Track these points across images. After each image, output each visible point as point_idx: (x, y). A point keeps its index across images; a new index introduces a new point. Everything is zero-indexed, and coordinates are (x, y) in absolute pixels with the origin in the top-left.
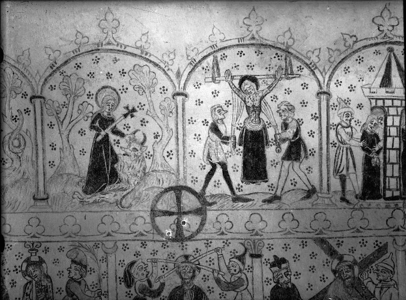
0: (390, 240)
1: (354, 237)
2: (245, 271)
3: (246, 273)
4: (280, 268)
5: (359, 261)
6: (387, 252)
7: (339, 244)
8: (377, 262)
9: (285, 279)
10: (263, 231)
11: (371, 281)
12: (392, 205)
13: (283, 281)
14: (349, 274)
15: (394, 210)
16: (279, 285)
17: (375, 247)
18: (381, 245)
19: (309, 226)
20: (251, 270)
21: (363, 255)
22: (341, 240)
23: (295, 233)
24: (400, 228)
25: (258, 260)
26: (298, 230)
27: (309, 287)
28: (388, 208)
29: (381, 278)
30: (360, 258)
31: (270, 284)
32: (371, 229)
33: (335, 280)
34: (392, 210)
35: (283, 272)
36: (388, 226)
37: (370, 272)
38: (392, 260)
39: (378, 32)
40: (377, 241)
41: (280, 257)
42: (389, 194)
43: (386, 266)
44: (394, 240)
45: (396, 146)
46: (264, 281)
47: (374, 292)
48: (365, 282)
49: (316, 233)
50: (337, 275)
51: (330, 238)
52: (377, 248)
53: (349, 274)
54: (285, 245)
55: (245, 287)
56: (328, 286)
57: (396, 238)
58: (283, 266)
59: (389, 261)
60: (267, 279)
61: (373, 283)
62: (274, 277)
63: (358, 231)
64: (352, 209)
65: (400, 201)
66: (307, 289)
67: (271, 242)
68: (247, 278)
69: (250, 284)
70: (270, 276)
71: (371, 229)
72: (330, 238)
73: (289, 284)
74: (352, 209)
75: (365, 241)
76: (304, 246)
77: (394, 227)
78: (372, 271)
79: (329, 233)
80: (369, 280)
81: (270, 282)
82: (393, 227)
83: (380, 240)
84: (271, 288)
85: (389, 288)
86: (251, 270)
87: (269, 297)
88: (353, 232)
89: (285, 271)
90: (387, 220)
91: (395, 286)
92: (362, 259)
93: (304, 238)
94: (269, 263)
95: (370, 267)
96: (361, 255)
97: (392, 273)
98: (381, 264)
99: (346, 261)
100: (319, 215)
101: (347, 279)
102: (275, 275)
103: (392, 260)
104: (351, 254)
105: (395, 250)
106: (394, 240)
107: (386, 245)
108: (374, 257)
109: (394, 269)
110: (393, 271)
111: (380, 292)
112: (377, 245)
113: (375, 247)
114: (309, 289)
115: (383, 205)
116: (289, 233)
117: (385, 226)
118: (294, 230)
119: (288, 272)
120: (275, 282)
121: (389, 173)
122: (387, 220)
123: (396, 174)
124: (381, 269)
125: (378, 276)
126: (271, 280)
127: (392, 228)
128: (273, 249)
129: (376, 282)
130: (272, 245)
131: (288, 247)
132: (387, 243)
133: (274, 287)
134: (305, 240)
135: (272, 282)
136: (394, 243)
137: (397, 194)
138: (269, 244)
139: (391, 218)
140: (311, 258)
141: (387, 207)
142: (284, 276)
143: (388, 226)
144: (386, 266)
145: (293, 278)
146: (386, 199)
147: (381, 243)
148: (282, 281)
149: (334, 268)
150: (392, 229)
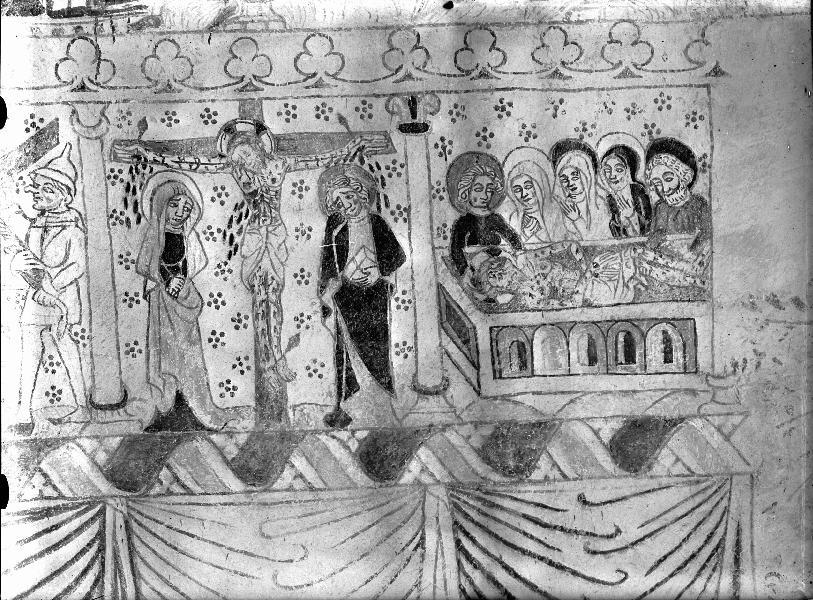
0: (62, 114)
6: (58, 143)
12: (69, 30)
15: (73, 42)
18: (42, 126)
24: (88, 84)
28: (58, 36)
29: (43, 204)
34: (68, 41)
38: (70, 162)
43: (56, 176)
44: (74, 112)
52: (33, 132)
59: (62, 164)
65: (86, 18)
83: (39, 112)
85: (64, 228)
90: (57, 65)
91: (80, 225)
97: (69, 193)
98: (42, 172)
103: (70, 162)
105: (76, 136)
107: (55, 124)
108: (27, 155)
109: (74, 183)
110: (73, 188)
111: (43, 239)
115: (47, 30)
122: (57, 65)
124: (41, 181)
125: (37, 199)
129: (33, 214)
132: (57, 119)
136: (75, 120)
139: (65, 59)
141: (57, 34)
144: (56, 176)
147: (42, 120)
150: (68, 88)
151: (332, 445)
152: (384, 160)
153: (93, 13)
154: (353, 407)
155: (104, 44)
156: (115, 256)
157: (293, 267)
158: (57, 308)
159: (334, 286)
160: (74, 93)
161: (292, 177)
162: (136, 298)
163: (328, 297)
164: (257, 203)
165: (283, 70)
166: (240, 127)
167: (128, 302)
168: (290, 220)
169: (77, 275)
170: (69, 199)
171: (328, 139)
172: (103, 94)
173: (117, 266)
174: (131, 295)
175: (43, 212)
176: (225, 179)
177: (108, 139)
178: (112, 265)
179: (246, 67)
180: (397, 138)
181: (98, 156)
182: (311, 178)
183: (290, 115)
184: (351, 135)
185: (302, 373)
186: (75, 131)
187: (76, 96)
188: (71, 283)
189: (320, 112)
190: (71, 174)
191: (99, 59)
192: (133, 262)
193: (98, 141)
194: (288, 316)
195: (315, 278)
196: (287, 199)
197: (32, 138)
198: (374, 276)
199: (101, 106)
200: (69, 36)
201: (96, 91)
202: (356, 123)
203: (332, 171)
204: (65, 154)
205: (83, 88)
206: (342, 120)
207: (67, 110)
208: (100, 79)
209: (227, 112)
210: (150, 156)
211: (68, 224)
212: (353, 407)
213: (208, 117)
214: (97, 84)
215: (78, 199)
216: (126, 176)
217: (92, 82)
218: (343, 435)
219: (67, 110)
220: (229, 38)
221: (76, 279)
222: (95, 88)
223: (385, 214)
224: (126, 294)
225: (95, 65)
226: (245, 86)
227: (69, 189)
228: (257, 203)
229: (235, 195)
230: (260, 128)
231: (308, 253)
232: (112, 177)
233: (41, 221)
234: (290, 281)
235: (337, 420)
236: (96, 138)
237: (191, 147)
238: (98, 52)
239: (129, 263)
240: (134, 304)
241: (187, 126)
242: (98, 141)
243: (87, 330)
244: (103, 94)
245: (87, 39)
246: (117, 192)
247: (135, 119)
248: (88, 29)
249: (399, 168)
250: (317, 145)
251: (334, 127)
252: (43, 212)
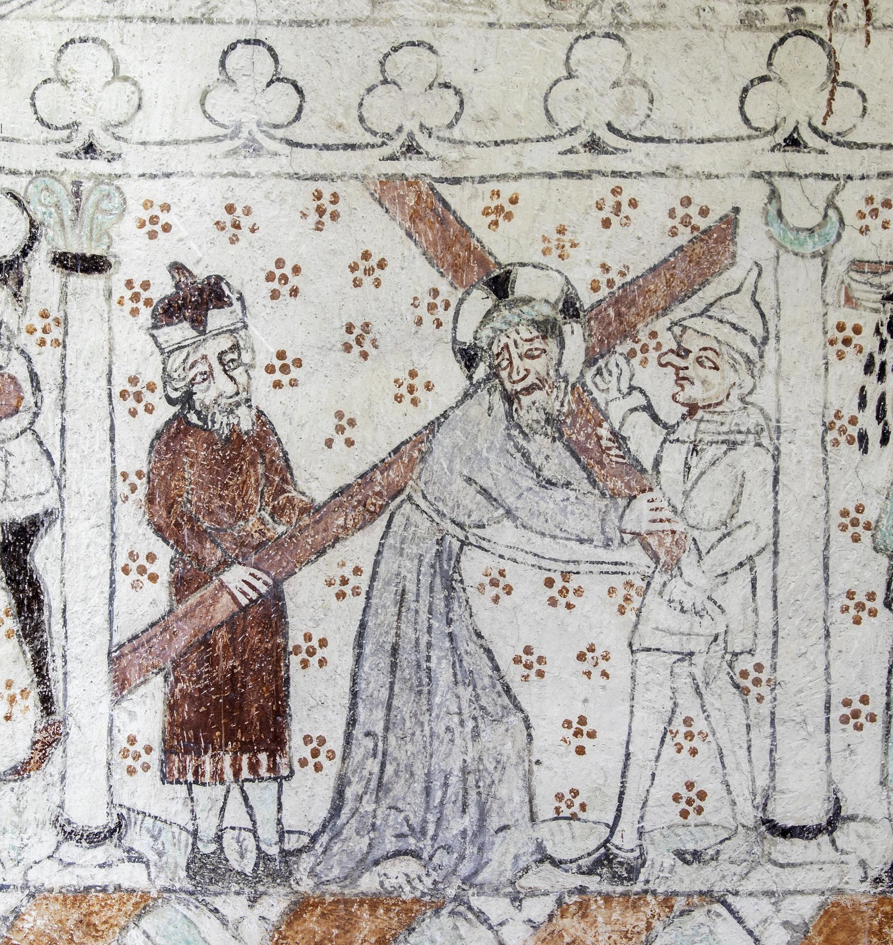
1: (569, 174)
2: (30, 343)
3: (33, 350)
4: (198, 323)
5: (587, 299)
7: (499, 209)
8: (678, 312)
9: (221, 383)
10: (121, 132)
11: (648, 408)
13: (212, 394)
14: (538, 366)
15: (782, 41)
16: (193, 418)
17: (674, 233)
19: (355, 114)
20: (57, 333)
21: (615, 268)
22: (507, 189)
23: (286, 149)
24: (806, 135)
25: (94, 282)
26: (298, 132)
27: (340, 429)
29: (694, 392)
30: (595, 288)
31: (149, 409)
32: (661, 140)
33: (467, 395)
34: (774, 38)
35: (213, 347)
36: (746, 121)
37: (644, 362)
38: (757, 305)
40: (687, 202)
41: (201, 273)
44: (774, 195)
46: (116, 392)
47: (657, 463)
48: (616, 412)
49: (386, 151)
50: (481, 372)
51: (456, 181)
52: (684, 236)
53: (538, 366)
54: (230, 209)
55: (23, 419)
56: (433, 426)
57: (782, 184)
58: (217, 318)
60: (133, 381)
61: (655, 418)
62: (167, 378)
63: (594, 145)
64: (569, 28)
66: (329, 443)
67: (158, 191)
68: (34, 377)
69: (50, 397)
70: (152, 373)
71: (661, 140)
72: (456, 181)
73: (242, 411)
74: (569, 28)
75: (624, 199)
76: (326, 218)
77: (775, 129)
78: (653, 355)
79: (453, 154)
80: (637, 399)
81: (148, 397)
82: (769, 127)
83: (701, 194)
84: (148, 436)
85: (733, 445)
86: (57, 333)
87: (139, 474)
88: (571, 151)
89: (225, 343)
92: (604, 292)
93: (324, 178)
94: (148, 302)
95: (643, 337)
96: (605, 268)
99: (527, 301)
100: (406, 56)
101: (529, 390)
102: (177, 360)
103: (757, 305)
104: (552, 260)
106: (774, 195)
112: (686, 221)
113: (674, 233)
114: (339, 440)
116: (254, 149)
117: (733, 125)
118: (280, 133)
119: (235, 347)
120: (171, 401)
124: (694, 343)
125: (681, 380)
126: (151, 387)
127: (767, 134)
128: (167, 228)
129: (670, 412)
130: (166, 208)
131: (246, 222)
133: (168, 423)
134: (327, 189)
135: (156, 398)
136: (773, 210)
138: (148, 205)
139: (764, 79)
140: (357, 283)
142: (217, 368)
143: (746, 121)
145: (261, 382)
148: (203, 395)
149: (465, 336)
150: (766, 142)
156: (835, 512)
158: (707, 618)
160: (778, 155)
162: (869, 605)
167: (853, 612)
169: (751, 548)
170: (748, 383)
173: (835, 533)
174: (860, 597)
175: (692, 409)
177: (840, 257)
178: (827, 530)
181: (814, 295)
186: (771, 238)
187: (778, 162)
188: (741, 565)
190: (758, 331)
191: (834, 80)
192: (868, 527)
193: (819, 260)
197: (681, 249)
199: (828, 186)
200: (774, 29)
201: (822, 152)
204: (748, 286)
205: (794, 142)
207: (761, 189)
208: (831, 127)
211: (740, 438)
214: (825, 137)
215: (767, 381)
217: (815, 130)
219: (761, 189)
221: (750, 558)
222: (819, 143)
224: (850, 595)
225: (826, 95)
227: (749, 361)
233: (687, 430)
236: (814, 256)
238: (834, 69)
239: (859, 529)
240: (864, 615)
242: (819, 260)
243: (767, 670)
245: (812, 37)
252: (692, 409)
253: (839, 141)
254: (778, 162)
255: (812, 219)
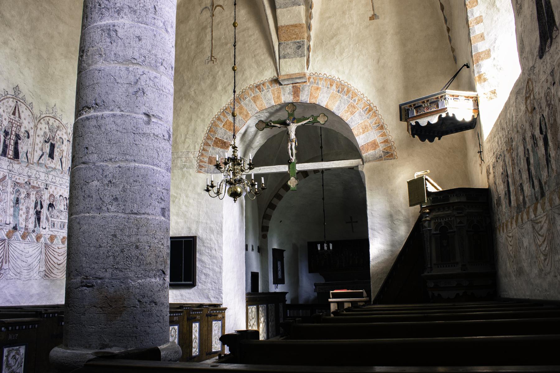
0: (7, 174)
29: (3, 188)
39: (14, 94)
42: (9, 156)
45: (14, 139)
59: (6, 183)
107: (6, 176)
115: (7, 160)
117: (6, 168)
121: (10, 149)
123: (12, 150)
137: (12, 157)
141: (8, 161)
146: (8, 158)
151: (33, 235)
152: (43, 192)
153: (13, 159)
154: (36, 229)
155: (14, 165)
157: (31, 206)
159: (36, 210)
161: (32, 192)
163: (35, 212)
164: (28, 195)
165: (33, 176)
166: (27, 183)
168: (32, 199)
171: (37, 188)
172: (13, 173)
176: (24, 190)
177: (12, 180)
179: (29, 174)
180: (44, 189)
182: (35, 193)
183: (33, 183)
184: (39, 187)
185: (31, 223)
187: (9, 172)
189: (37, 183)
194: (30, 214)
195: (34, 208)
196: (31, 196)
198: (40, 210)
202: (40, 186)
203: (37, 192)
205: (10, 171)
206: (39, 185)
209: (26, 180)
210: (16, 184)
212: (36, 229)
213: (24, 180)
216: (13, 186)
218: (34, 234)
220: (28, 169)
223: (42, 200)
226: (29, 177)
228: (28, 195)
229: (26, 193)
230: (30, 184)
231: (33, 205)
232: (12, 186)
234: (31, 208)
235: (34, 231)
237: (21, 184)
241: (21, 181)
244: (13, 173)
246: (12, 188)
247: (15, 178)
248: (12, 162)
249: (44, 194)
250: (36, 188)
251: (38, 186)
253: (13, 171)
254: (9, 172)
255: (11, 177)
